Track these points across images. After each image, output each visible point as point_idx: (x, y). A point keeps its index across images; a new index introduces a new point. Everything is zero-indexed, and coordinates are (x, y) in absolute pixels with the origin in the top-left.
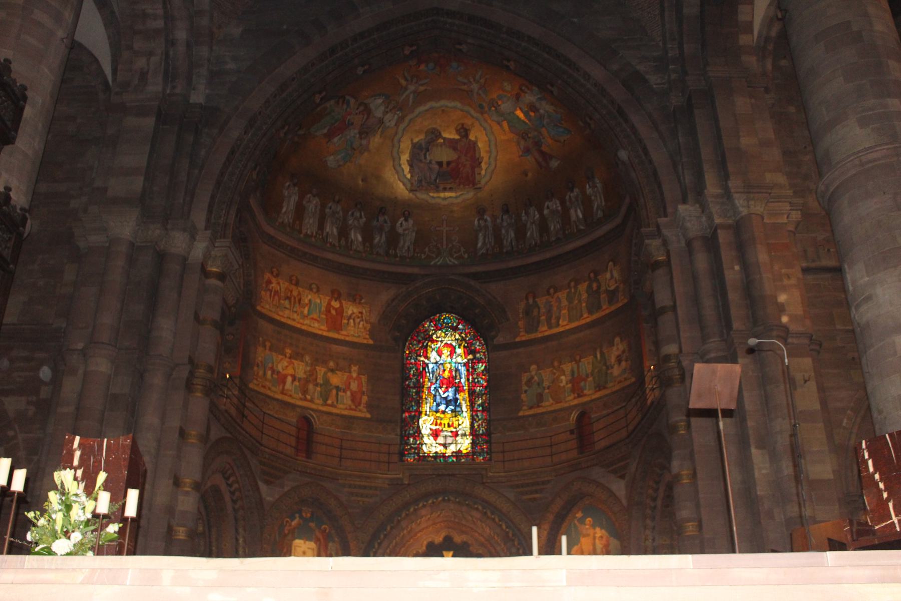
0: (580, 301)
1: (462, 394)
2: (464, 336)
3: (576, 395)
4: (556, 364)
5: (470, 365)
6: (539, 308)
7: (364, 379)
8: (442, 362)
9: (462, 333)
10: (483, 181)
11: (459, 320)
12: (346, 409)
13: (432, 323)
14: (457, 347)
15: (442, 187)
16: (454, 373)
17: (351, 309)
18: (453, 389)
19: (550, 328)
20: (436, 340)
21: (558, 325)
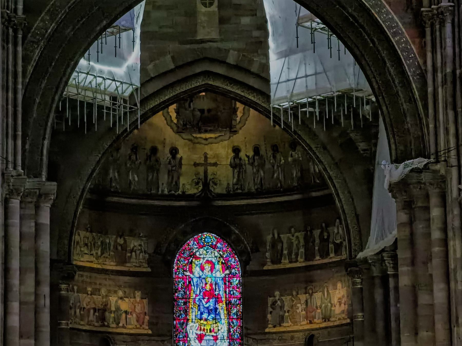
0: (314, 245)
1: (221, 304)
2: (222, 254)
3: (308, 322)
4: (294, 293)
5: (227, 279)
6: (282, 243)
7: (145, 301)
8: (204, 276)
9: (220, 251)
10: (238, 127)
11: (217, 239)
12: (134, 328)
13: (195, 242)
14: (216, 263)
15: (203, 128)
16: (214, 286)
17: (134, 243)
18: (213, 300)
19: (291, 262)
20: (199, 257)
21: (297, 261)
